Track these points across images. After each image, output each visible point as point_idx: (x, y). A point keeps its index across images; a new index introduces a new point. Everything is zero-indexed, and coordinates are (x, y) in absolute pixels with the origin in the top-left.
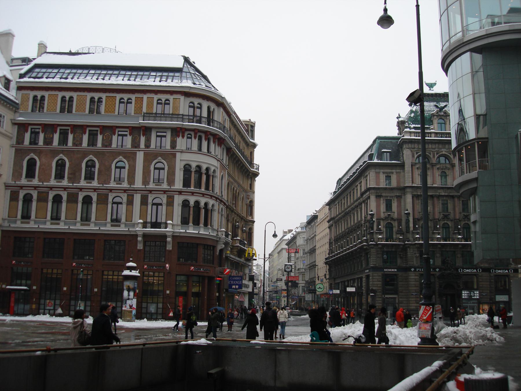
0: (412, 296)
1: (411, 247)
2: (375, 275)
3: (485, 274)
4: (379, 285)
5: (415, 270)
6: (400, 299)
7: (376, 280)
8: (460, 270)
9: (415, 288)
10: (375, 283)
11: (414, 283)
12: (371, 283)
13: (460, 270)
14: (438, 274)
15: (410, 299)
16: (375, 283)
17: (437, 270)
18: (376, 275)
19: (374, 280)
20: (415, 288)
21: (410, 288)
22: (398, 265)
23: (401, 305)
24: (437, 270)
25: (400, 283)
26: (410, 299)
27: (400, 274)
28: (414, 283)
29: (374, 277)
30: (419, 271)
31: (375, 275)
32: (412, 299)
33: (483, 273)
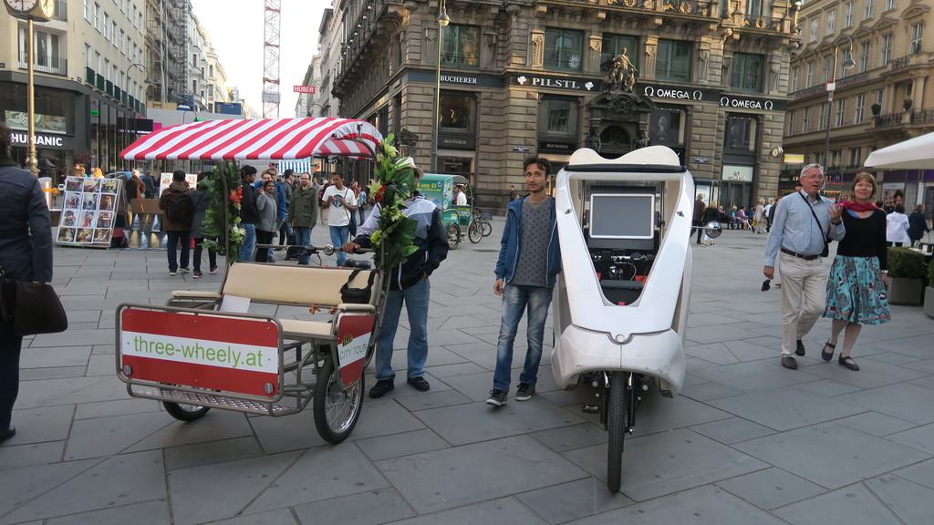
0: (515, 156)
1: (523, 13)
2: (416, 90)
3: (710, 106)
4: (425, 122)
5: (529, 83)
6: (481, 163)
7: (419, 106)
8: (649, 91)
9: (523, 134)
10: (415, 114)
11: (522, 118)
12: (403, 115)
13: (649, 91)
14: (589, 98)
15: (509, 164)
16: (415, 114)
17: (589, 85)
18: (420, 91)
19: (412, 105)
20: (523, 134)
21: (512, 133)
22: (482, 66)
23: (481, 178)
24: (589, 85)
25: (483, 118)
26: (509, 164)
27: (485, 92)
28: (522, 118)
29: (414, 98)
30: (538, 84)
31: (416, 90)
32: (515, 164)
33: (705, 104)
